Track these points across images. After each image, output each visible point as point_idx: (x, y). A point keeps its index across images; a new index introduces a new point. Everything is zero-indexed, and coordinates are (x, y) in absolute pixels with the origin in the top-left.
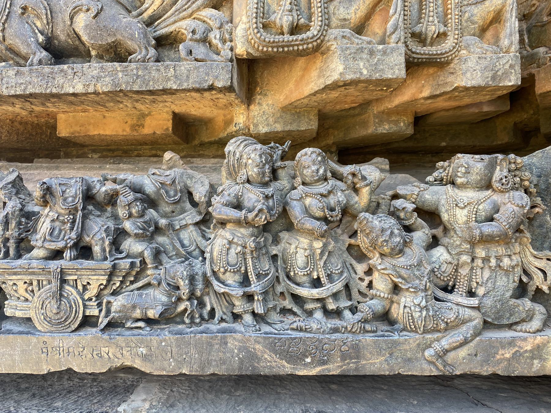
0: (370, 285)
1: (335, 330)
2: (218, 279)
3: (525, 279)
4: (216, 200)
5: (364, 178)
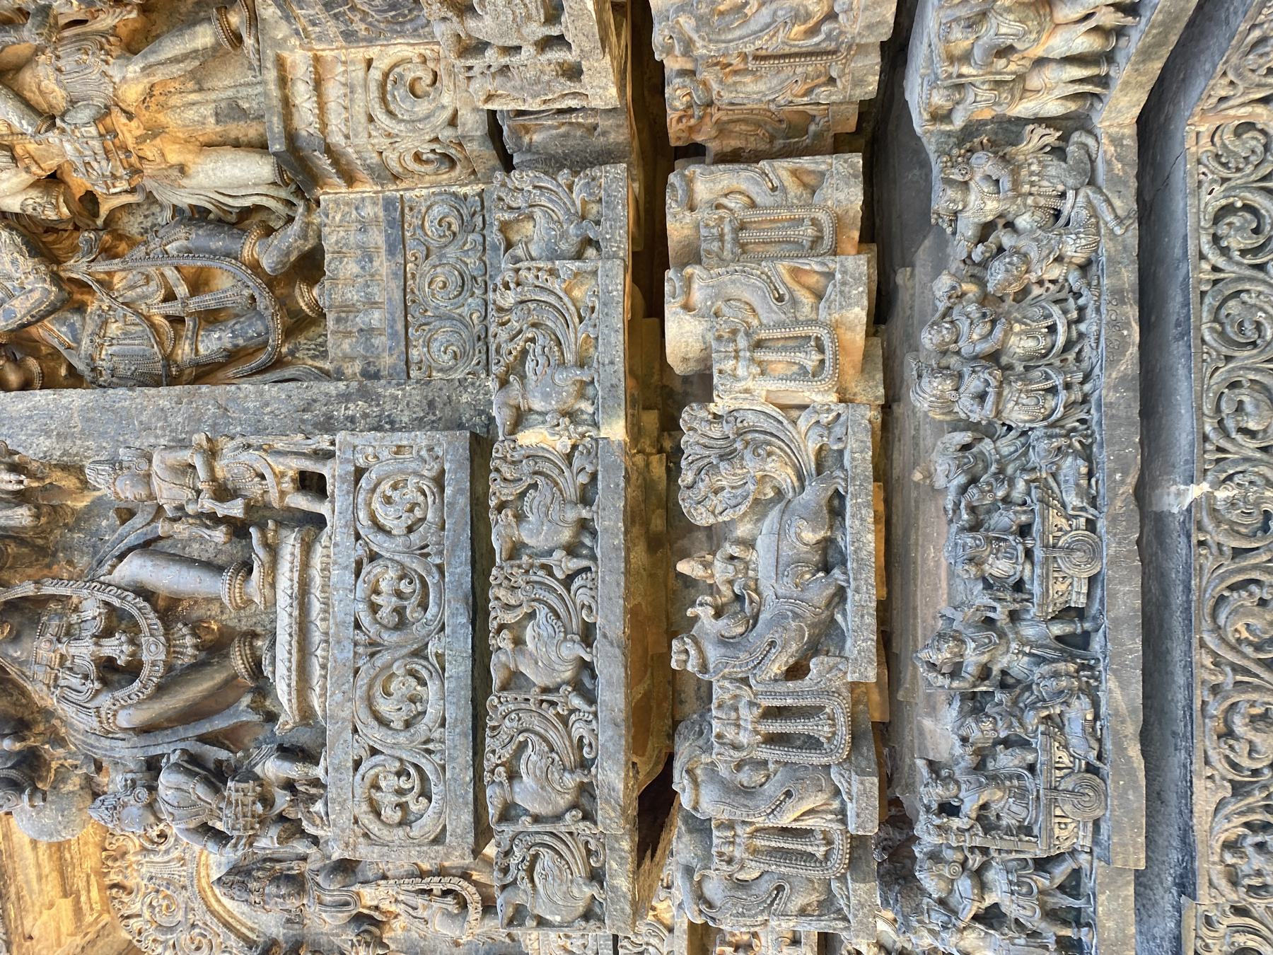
0: (1053, 282)
1: (1098, 310)
2: (1050, 415)
3: (1048, 149)
4: (975, 418)
5: (954, 288)
